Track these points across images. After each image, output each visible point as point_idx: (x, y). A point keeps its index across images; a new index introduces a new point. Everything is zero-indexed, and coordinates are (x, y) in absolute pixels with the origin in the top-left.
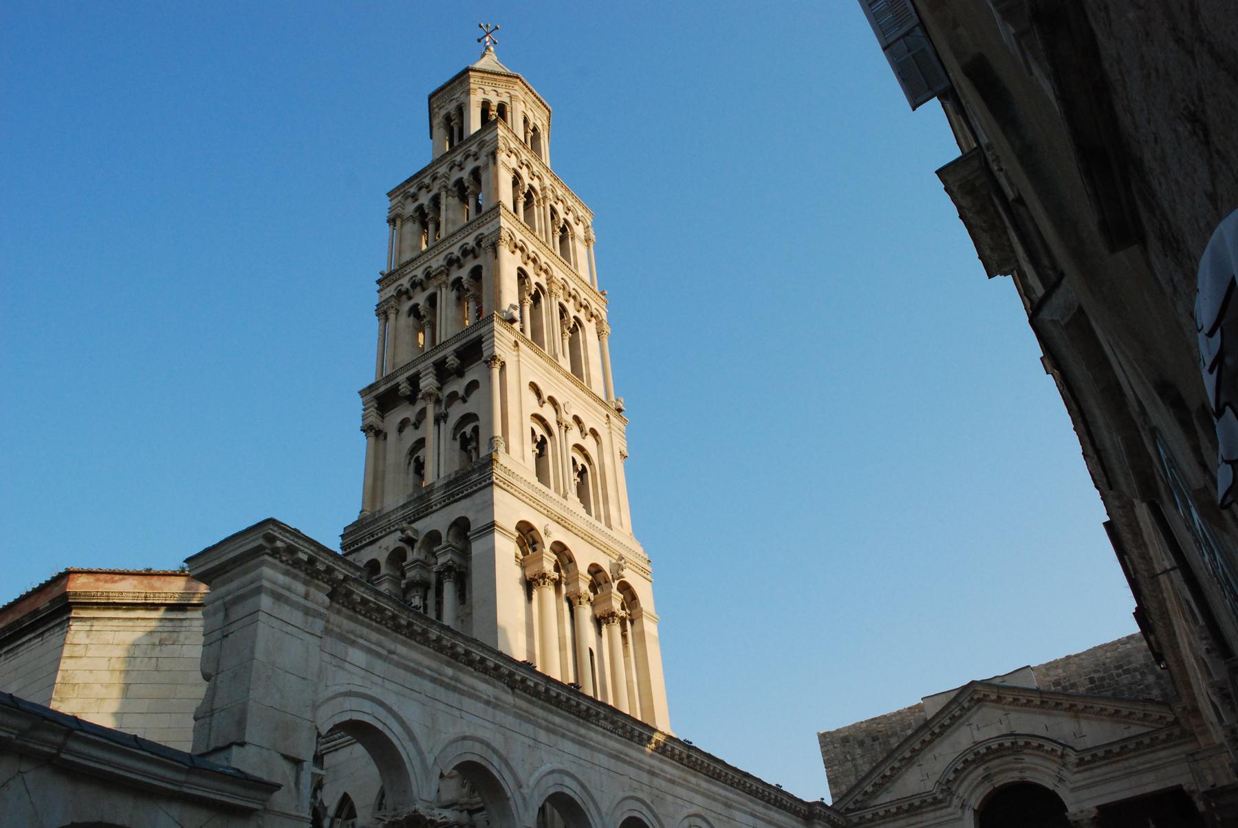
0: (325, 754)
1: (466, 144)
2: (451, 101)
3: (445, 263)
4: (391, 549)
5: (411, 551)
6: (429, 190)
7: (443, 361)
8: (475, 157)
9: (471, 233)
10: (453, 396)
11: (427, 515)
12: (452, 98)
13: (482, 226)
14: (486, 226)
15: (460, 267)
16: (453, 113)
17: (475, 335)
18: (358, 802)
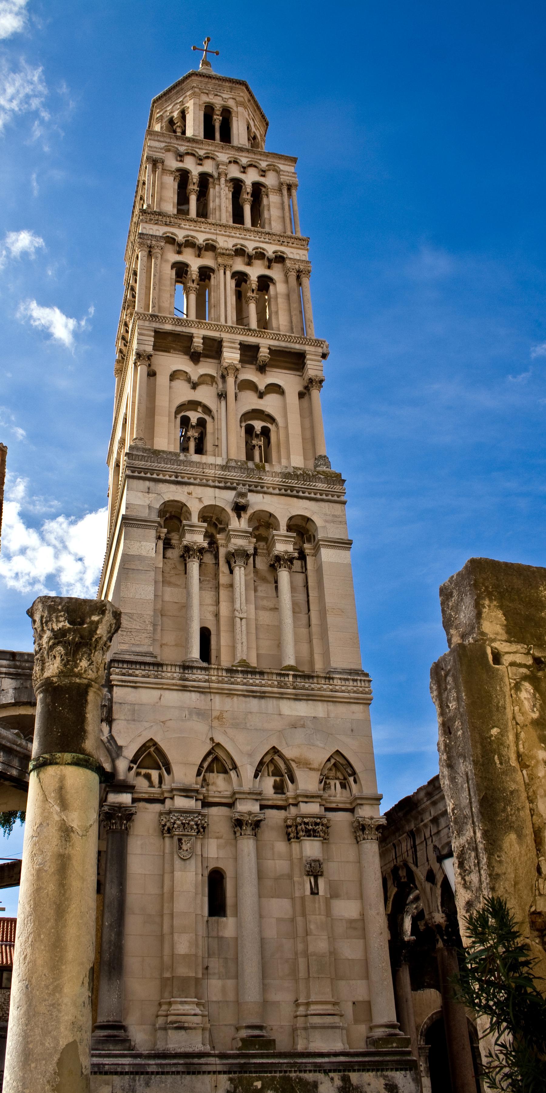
0: (117, 685)
1: (255, 154)
2: (217, 95)
3: (234, 248)
4: (208, 502)
5: (237, 519)
6: (200, 160)
7: (256, 348)
8: (264, 174)
9: (271, 243)
10: (249, 385)
11: (258, 492)
12: (219, 94)
13: (285, 246)
14: (292, 250)
15: (249, 264)
16: (218, 108)
17: (297, 346)
18: (171, 755)
